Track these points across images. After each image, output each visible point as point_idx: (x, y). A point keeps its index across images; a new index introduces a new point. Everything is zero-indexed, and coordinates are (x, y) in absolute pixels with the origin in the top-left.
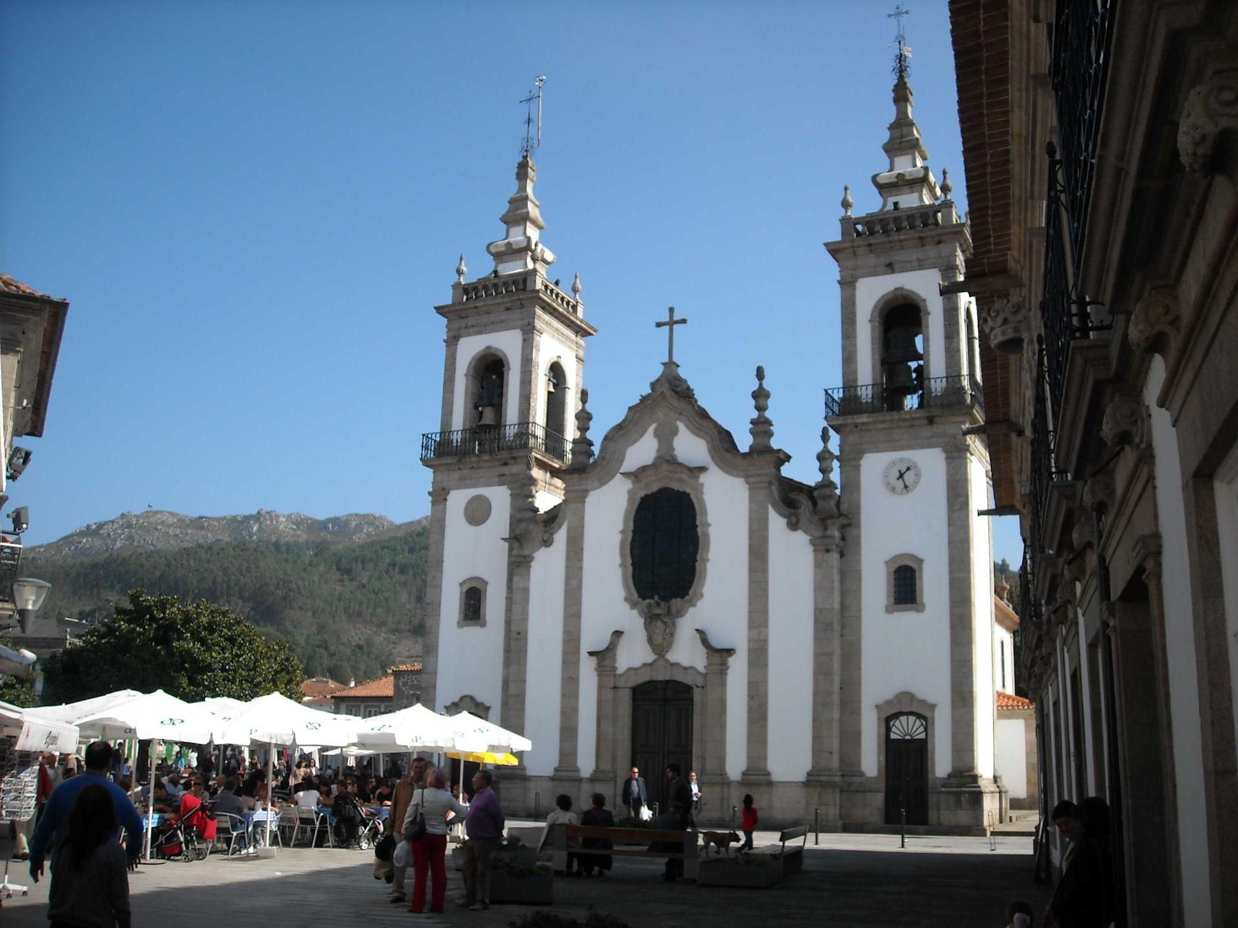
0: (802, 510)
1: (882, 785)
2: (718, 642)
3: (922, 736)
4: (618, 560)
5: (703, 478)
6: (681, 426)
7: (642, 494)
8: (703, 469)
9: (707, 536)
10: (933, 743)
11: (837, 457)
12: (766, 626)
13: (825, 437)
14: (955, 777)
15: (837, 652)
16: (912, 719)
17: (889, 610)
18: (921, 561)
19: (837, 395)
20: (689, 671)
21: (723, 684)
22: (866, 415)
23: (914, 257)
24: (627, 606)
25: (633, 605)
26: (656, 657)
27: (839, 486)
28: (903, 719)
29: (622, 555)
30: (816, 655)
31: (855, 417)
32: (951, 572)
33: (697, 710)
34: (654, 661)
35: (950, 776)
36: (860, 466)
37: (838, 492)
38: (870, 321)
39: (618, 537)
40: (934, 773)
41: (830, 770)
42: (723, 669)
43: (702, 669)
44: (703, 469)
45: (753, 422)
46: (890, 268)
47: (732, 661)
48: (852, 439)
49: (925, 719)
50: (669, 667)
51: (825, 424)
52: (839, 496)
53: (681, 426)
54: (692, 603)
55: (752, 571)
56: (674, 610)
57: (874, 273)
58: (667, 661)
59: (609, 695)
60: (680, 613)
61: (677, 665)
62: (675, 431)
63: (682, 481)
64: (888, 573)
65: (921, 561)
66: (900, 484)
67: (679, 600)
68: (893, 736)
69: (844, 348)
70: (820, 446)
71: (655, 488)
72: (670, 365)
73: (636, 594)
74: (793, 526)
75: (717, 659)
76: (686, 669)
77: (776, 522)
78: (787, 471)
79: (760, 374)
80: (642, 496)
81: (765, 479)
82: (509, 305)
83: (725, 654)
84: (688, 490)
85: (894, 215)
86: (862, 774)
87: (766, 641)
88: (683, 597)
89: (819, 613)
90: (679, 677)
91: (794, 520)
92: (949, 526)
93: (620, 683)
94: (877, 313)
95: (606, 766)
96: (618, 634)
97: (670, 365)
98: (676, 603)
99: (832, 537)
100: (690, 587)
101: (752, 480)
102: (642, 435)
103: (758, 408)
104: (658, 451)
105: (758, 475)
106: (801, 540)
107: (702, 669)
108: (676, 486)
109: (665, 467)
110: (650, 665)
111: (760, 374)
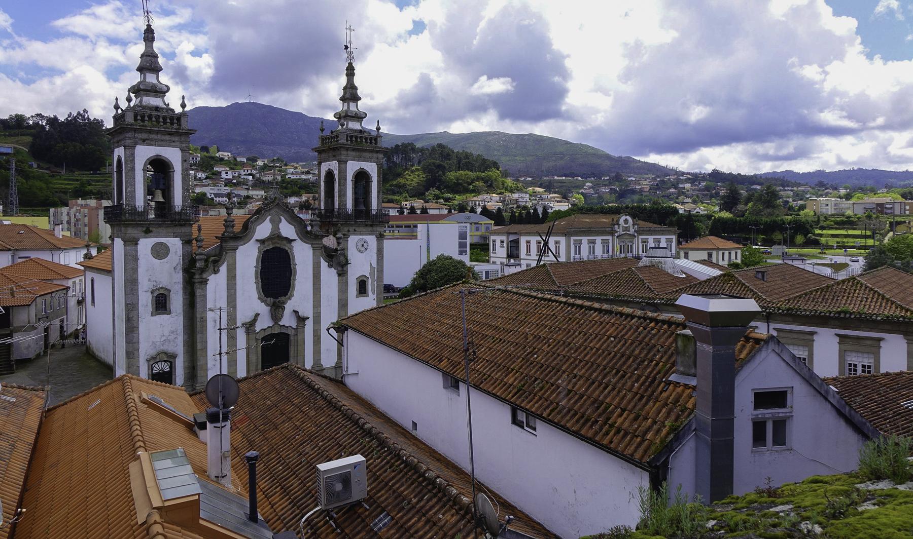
5: (293, 244)
6: (282, 218)
9: (295, 269)
24: (259, 301)
25: (262, 301)
29: (256, 278)
34: (273, 325)
43: (294, 326)
47: (307, 322)
53: (282, 218)
54: (290, 299)
61: (284, 326)
62: (280, 221)
66: (363, 249)
73: (264, 296)
74: (330, 266)
76: (287, 327)
77: (324, 264)
84: (287, 248)
90: (284, 331)
91: (331, 263)
96: (257, 315)
106: (333, 272)
107: (294, 326)
110: (271, 327)
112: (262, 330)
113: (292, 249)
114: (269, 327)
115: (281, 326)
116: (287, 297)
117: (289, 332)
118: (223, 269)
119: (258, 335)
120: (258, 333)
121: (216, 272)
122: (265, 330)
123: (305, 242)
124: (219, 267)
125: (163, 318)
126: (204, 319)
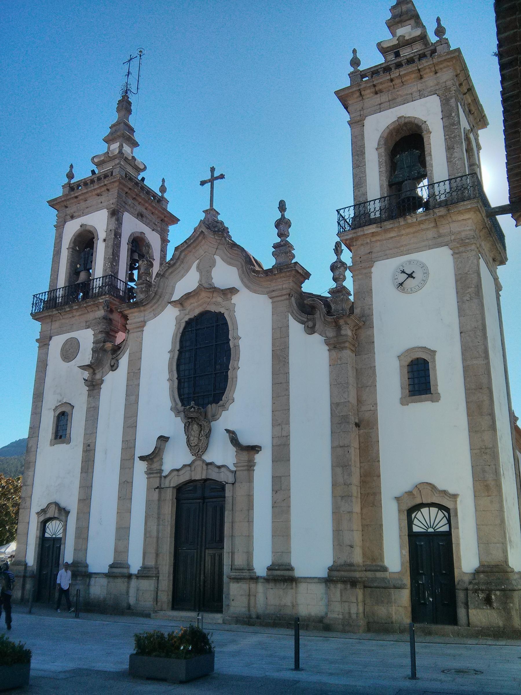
0: (317, 315)
1: (407, 580)
2: (245, 440)
3: (446, 528)
4: (167, 376)
5: (235, 299)
6: (217, 258)
7: (187, 318)
8: (233, 291)
9: (237, 347)
10: (458, 537)
11: (351, 269)
12: (288, 423)
13: (338, 250)
14: (483, 572)
15: (355, 444)
16: (434, 510)
17: (404, 402)
18: (433, 353)
19: (349, 214)
20: (223, 469)
21: (250, 480)
22: (375, 225)
23: (415, 89)
24: (173, 414)
25: (178, 413)
26: (194, 458)
27: (353, 294)
28: (425, 510)
29: (170, 371)
30: (333, 448)
31: (365, 228)
32: (464, 360)
33: (228, 506)
34: (193, 462)
35: (477, 572)
36: (371, 273)
37: (351, 298)
38: (377, 149)
39: (167, 356)
40: (460, 568)
41: (351, 565)
42: (250, 466)
44: (233, 291)
45: (276, 246)
46: (393, 103)
47: (259, 458)
48: (363, 250)
49: (447, 510)
50: (205, 467)
51: (338, 239)
52: (353, 303)
53: (217, 258)
54: (224, 407)
55: (275, 373)
56: (209, 415)
57: (380, 108)
58: (204, 461)
59: (155, 495)
60: (215, 418)
61: (211, 464)
62: (213, 264)
63: (216, 304)
64: (401, 366)
65: (433, 353)
67: (214, 405)
68: (415, 529)
69: (355, 176)
70: (334, 258)
71: (197, 312)
72: (211, 212)
73: (180, 404)
74: (311, 330)
75: (245, 456)
76: (219, 467)
78: (307, 287)
79: (282, 207)
80: (187, 320)
81: (284, 292)
82: (99, 191)
83: (252, 453)
84: (222, 310)
85: (395, 61)
86: (384, 569)
87: (288, 436)
88: (217, 403)
89: (334, 406)
90: (214, 475)
91: (310, 324)
92: (460, 316)
93: (166, 483)
94: (382, 142)
95: (151, 563)
96: (163, 439)
97: (211, 212)
98: (211, 408)
99: (346, 335)
100: (223, 393)
101: (274, 294)
102: (187, 271)
103: (280, 235)
104: (200, 280)
105: (280, 290)
108: (213, 308)
109: (203, 294)
110: (190, 465)
111: (282, 207)
112: (173, 471)
113: (232, 309)
114: (185, 466)
115: (208, 464)
116: (221, 403)
117: (223, 477)
118: (124, 361)
119: (168, 480)
120: (165, 477)
121: (114, 367)
122: (178, 470)
123: (255, 292)
124: (117, 361)
125: (62, 447)
126: (92, 445)
